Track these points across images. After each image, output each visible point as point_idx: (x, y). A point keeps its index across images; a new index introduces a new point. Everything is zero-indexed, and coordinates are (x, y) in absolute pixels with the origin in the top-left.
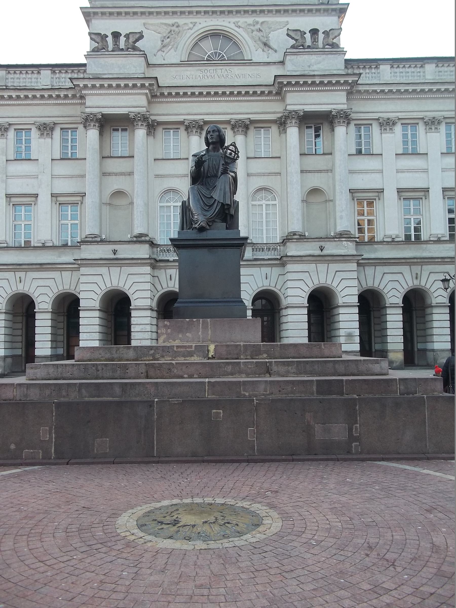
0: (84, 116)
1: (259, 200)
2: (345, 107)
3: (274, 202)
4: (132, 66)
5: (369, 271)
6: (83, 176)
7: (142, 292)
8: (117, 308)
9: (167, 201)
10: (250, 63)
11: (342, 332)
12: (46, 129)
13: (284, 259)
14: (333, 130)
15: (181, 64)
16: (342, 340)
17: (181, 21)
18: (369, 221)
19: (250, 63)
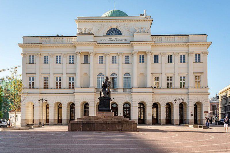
0: (76, 52)
1: (126, 76)
2: (150, 50)
3: (130, 77)
4: (91, 39)
5: (157, 96)
6: (76, 68)
7: (93, 101)
8: (86, 106)
9: (100, 76)
10: (124, 36)
11: (147, 114)
12: (65, 55)
13: (132, 93)
14: (147, 57)
15: (104, 36)
16: (147, 116)
17: (104, 23)
18: (157, 82)
19: (124, 36)
